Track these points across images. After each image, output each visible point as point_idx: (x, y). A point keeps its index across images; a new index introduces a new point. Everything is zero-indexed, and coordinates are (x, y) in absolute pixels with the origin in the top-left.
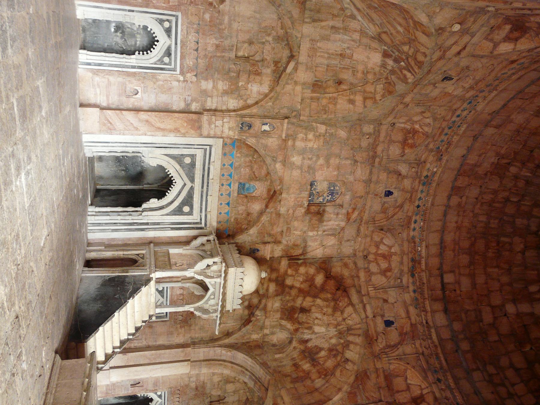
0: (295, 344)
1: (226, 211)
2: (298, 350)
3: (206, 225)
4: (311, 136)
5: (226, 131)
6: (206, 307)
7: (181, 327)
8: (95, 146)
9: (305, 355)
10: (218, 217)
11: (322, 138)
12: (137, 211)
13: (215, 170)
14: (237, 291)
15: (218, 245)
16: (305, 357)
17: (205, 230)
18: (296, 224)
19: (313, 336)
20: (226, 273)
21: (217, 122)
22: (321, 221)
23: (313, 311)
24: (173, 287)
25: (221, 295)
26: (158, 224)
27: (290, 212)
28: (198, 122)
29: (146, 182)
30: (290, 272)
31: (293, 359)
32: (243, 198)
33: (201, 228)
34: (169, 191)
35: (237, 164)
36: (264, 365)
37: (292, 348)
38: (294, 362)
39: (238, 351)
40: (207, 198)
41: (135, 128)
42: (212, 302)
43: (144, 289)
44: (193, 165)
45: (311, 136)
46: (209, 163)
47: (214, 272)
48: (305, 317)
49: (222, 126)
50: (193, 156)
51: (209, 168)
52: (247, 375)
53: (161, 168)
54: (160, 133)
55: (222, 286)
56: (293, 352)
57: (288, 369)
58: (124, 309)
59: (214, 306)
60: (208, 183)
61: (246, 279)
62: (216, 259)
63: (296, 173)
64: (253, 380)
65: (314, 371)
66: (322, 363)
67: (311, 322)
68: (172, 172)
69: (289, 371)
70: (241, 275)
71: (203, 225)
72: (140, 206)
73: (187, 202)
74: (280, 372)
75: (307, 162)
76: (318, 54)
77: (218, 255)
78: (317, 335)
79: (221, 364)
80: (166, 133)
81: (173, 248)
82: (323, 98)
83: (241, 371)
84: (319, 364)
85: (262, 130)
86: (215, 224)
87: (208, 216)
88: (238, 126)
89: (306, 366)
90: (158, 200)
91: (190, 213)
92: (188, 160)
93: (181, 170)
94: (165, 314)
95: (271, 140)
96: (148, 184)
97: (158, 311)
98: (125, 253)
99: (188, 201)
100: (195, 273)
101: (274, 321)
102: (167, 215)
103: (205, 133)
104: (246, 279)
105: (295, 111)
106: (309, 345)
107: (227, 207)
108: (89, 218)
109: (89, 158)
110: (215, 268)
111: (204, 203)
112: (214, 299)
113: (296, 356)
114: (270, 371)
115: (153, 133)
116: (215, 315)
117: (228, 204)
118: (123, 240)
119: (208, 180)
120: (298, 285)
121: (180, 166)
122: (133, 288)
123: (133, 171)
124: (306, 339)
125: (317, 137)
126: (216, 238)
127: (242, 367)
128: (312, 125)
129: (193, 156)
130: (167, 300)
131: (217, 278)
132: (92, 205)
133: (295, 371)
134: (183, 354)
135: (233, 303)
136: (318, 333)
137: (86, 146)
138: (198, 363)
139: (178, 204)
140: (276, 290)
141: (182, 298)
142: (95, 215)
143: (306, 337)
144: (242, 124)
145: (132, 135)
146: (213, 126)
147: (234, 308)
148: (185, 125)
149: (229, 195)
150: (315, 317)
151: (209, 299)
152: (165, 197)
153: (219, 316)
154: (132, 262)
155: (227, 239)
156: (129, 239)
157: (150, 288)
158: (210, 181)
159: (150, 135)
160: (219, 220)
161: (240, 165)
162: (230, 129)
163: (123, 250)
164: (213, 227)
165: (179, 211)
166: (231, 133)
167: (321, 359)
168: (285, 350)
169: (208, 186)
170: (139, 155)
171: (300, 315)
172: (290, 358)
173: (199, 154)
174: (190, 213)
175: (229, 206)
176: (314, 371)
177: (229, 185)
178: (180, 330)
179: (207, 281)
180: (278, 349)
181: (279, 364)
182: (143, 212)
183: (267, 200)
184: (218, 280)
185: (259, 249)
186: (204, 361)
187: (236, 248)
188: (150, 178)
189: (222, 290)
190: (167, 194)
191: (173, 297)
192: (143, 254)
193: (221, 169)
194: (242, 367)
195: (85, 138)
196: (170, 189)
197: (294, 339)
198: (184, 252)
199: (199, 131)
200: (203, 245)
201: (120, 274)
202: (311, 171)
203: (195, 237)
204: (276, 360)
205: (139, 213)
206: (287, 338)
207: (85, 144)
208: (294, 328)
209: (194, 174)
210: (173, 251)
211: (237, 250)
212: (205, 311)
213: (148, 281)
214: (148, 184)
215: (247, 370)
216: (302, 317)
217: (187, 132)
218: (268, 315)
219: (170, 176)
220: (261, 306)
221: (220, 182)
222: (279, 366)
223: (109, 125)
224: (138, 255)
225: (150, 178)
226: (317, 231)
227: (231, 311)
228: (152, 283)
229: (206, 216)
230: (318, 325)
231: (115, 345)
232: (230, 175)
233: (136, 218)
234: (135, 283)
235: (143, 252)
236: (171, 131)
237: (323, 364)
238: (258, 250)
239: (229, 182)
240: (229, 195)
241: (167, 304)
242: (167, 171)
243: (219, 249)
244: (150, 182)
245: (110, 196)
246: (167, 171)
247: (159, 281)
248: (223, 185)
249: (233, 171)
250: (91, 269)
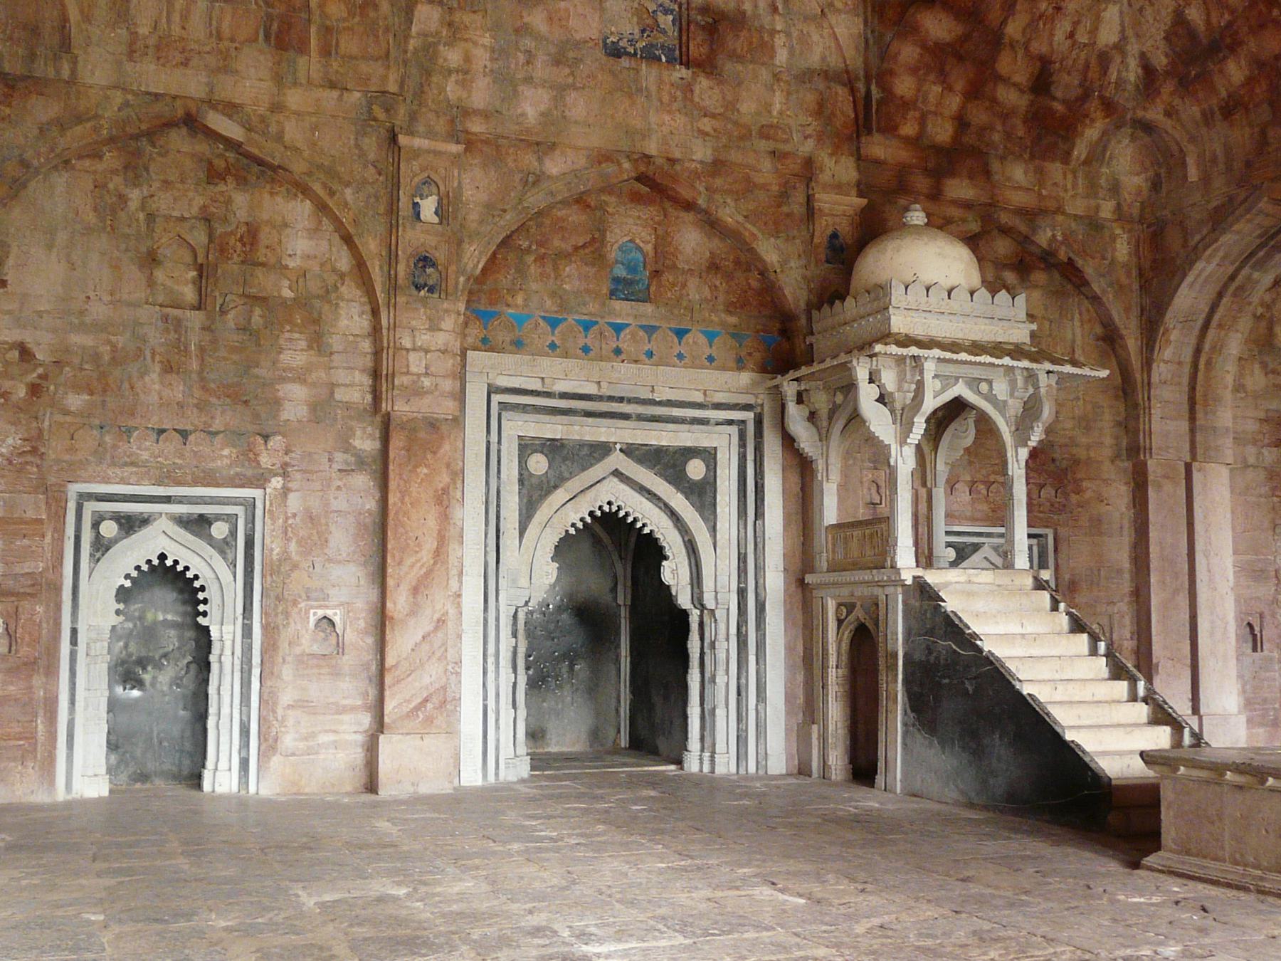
0: (1155, 114)
1: (702, 340)
2: (1177, 101)
3: (747, 407)
4: (453, 57)
5: (441, 339)
6: (1015, 407)
7: (1078, 491)
8: (497, 748)
9: (1197, 76)
10: (724, 368)
11: (457, 17)
12: (701, 625)
13: (569, 376)
14: (968, 306)
15: (816, 367)
16: (1204, 78)
17: (766, 408)
18: (747, 107)
19: (1133, 48)
20: (906, 341)
21: (413, 369)
22: (738, 21)
23: (1044, 49)
24: (947, 516)
25: (978, 359)
26: (742, 559)
27: (708, 129)
28: (414, 430)
29: (609, 598)
30: (909, 129)
31: (1207, 118)
32: (660, 285)
33: (759, 422)
34: (639, 525)
35: (549, 303)
36: (1219, 219)
37: (1167, 124)
38: (1218, 116)
39: (1169, 304)
40: (660, 403)
41: (436, 628)
42: (1001, 389)
43: (951, 604)
44: (553, 448)
45: (453, 57)
46: (548, 395)
47: (901, 380)
48: (1065, 78)
49: (427, 351)
50: (526, 447)
51: (564, 396)
52: (1249, 278)
53: (564, 548)
54: (453, 550)
55: (948, 355)
56: (1184, 117)
57: (1240, 135)
58: (1012, 666)
59: (1013, 384)
60: (611, 399)
61: (929, 275)
62: (862, 373)
63: (578, 106)
64: (1269, 256)
65: (1252, 45)
66: (1227, 17)
67: (1083, 55)
68: (577, 514)
69: (1247, 130)
70: (917, 292)
71: (749, 416)
72: (685, 614)
73: (674, 466)
74: (1248, 164)
75: (541, 69)
76: (176, 30)
77: (846, 368)
78: (1130, 32)
79: (1209, 363)
80: (453, 532)
81: (821, 511)
82: (324, 15)
83: (1235, 295)
84: (1230, 24)
85: (436, 220)
86: (745, 378)
87: (720, 398)
88: (424, 301)
89: (1235, 71)
90: (666, 558)
91: (709, 456)
92: (538, 464)
93: (569, 484)
94: (1034, 541)
95: (468, 193)
96: (614, 590)
97: (1022, 561)
98: (832, 661)
99: (670, 463)
100: (903, 442)
101: (1075, 186)
102: (713, 530)
103: (449, 406)
104: (928, 276)
105: (370, 110)
106: (1160, 60)
107: (689, 338)
108: (720, 770)
109: (533, 768)
110: (889, 379)
111: (677, 412)
112: (990, 382)
113: (1196, 110)
114: (1243, 195)
115: (454, 572)
116: (1043, 380)
117: (680, 333)
118: (790, 668)
119: (600, 398)
120: (954, 103)
121: (556, 487)
122: (945, 637)
123: (575, 638)
124: (1140, 70)
125: (455, 32)
126: (793, 374)
127: (1220, 295)
128: (416, 50)
129: (526, 447)
130: (989, 535)
131: (921, 373)
132: (679, 762)
133: (1247, 109)
134: (1168, 487)
135: (1009, 319)
136: (1123, 31)
137: (497, 774)
138: (1199, 438)
139: (680, 496)
140: (970, 178)
141: (981, 487)
142: (713, 752)
143: (1133, 72)
144: (418, 288)
145: (460, 637)
146: (426, 382)
147: (1022, 315)
148: (425, 471)
149: (651, 330)
150: (1069, 42)
151: (991, 398)
152: (658, 536)
153: (1048, 366)
154: (864, 642)
155: (796, 335)
156: (789, 649)
157: (947, 585)
158: (605, 391)
159: (461, 582)
160: (732, 364)
161: (553, 294)
162: (434, 328)
163: (825, 667)
164: (755, 384)
165: (703, 494)
166: (448, 323)
167: (1214, 20)
168: (1175, 148)
169: (621, 400)
170: (521, 616)
171: (1059, 94)
172: (1204, 130)
173: (517, 427)
174: (709, 456)
175: (687, 331)
176: (1252, 45)
177: (618, 328)
178: (1088, 494)
179: (931, 403)
180: (1169, 172)
181: (1222, 166)
182: (702, 607)
183: (667, 204)
184: (930, 368)
185: (829, 232)
186: (1192, 418)
187: (826, 307)
188: (595, 584)
189: (963, 356)
190: (646, 531)
191: (978, 515)
192: (839, 605)
193: (566, 355)
194: (1220, 295)
195: (471, 777)
196: (630, 519)
197: (1140, 114)
198: (835, 476)
199: (444, 428)
200: (812, 417)
201: (900, 677)
202: (571, 54)
203: (789, 441)
204: (1206, 180)
205: (706, 619)
206: (1133, 138)
207: (491, 778)
208: (1099, 114)
209: (582, 444)
210: (830, 512)
211: (832, 304)
212: (1030, 410)
213: (924, 591)
214: (614, 590)
215: (1232, 278)
216: (1066, 85)
217: (448, 465)
218: (1052, 205)
219: (589, 520)
220: (1023, 228)
221: (608, 360)
222: (1229, 169)
223: (429, 706)
224: (840, 622)
225: (595, 584)
226: (773, 32)
227: (1034, 327)
228: (932, 577)
229: (718, 406)
230: (1094, 31)
231: (1125, 696)
232: (587, 326)
233: (722, 626)
234: (931, 632)
235: (831, 605)
236: (445, 517)
237: (1232, 12)
238: (834, 236)
239: (609, 332)
240: (651, 330)
241: (1002, 535)
242: (572, 531)
243: (829, 363)
244: (609, 584)
245: (651, 708)
246: (572, 531)
247: (926, 558)
248: (618, 351)
249: (571, 319)
250: (881, 764)
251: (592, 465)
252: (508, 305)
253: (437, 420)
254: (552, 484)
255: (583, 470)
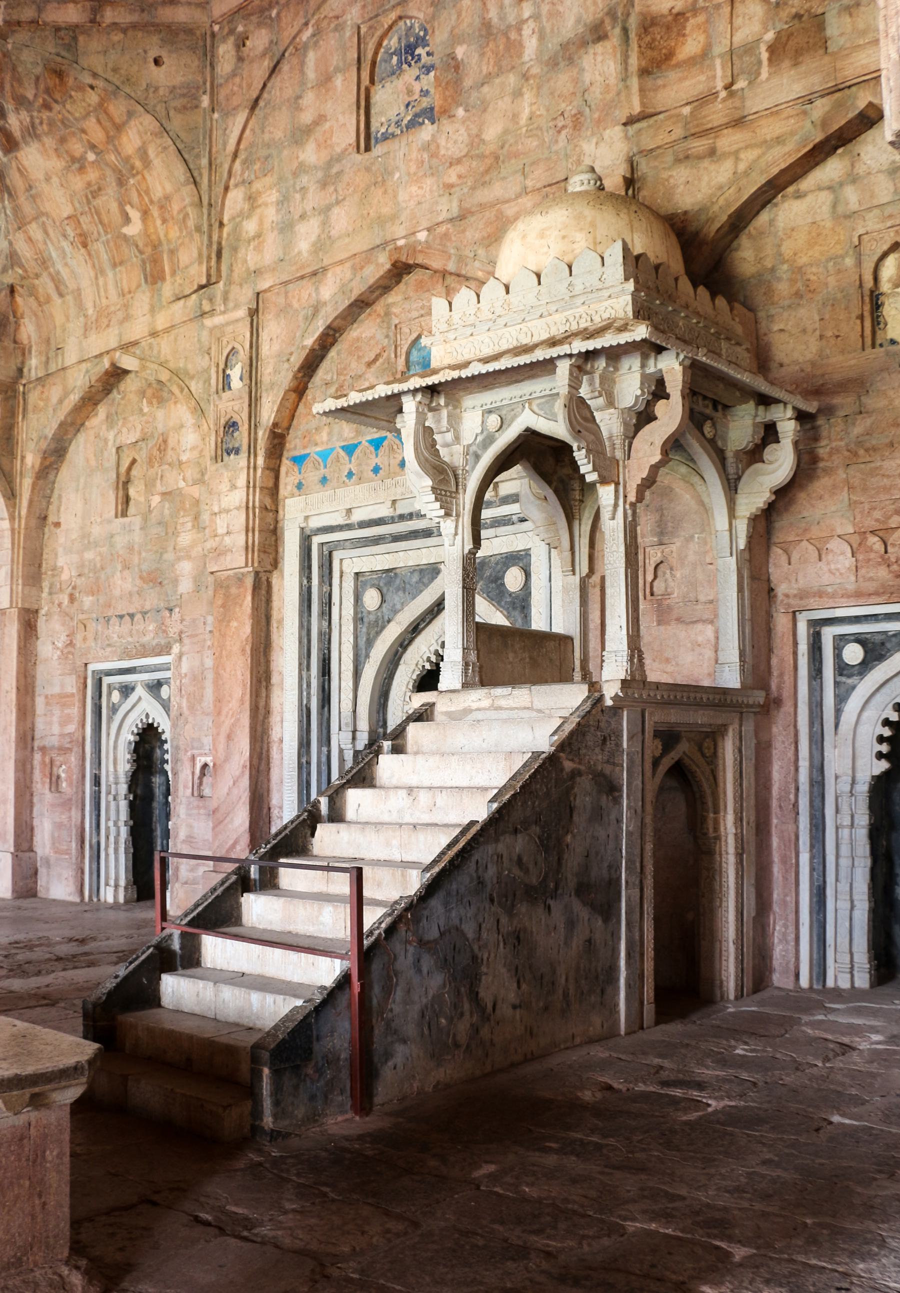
27: (453, 179)
28: (228, 587)
46: (349, 527)
51: (363, 525)
63: (341, 219)
76: (104, 301)
82: (169, 241)
119: (392, 520)
121: (389, 621)
141: (874, 541)
191: (871, 586)
251: (421, 591)
252: (316, 444)
253: (242, 574)
254: (386, 618)
255: (414, 598)
